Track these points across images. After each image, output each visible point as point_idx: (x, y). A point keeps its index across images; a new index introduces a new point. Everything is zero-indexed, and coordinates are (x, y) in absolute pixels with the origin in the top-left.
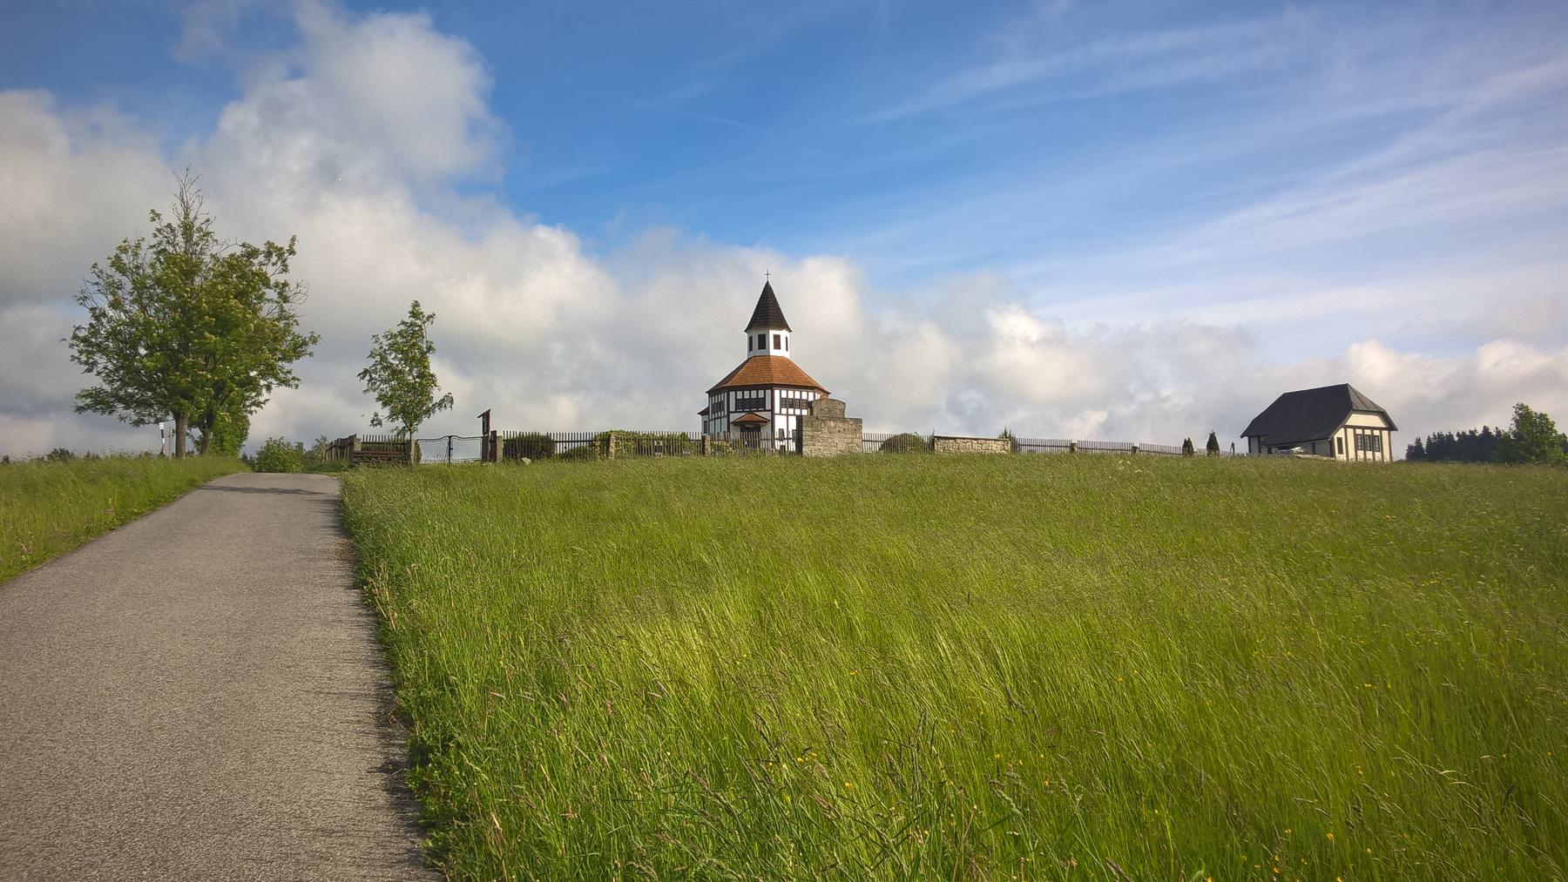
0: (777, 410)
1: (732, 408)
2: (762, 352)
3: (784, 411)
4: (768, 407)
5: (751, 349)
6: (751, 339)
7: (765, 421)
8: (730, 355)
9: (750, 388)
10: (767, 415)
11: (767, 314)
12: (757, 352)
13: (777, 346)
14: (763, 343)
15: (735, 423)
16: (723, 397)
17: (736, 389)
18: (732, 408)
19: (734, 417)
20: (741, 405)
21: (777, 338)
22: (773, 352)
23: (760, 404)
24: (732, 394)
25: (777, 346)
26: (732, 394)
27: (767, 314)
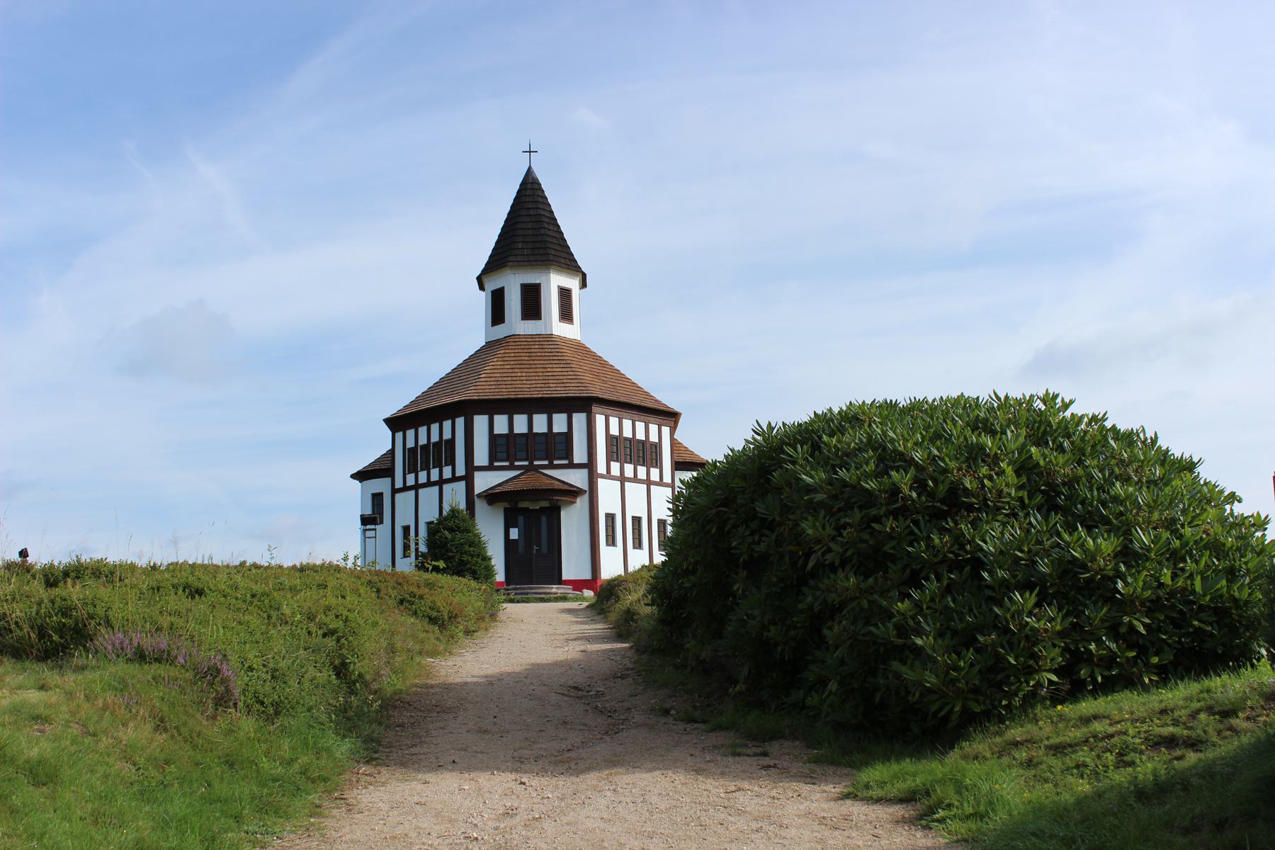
0: (601, 468)
1: (481, 457)
2: (530, 327)
3: (615, 467)
4: (579, 455)
5: (498, 315)
7: (572, 493)
8: (444, 325)
9: (530, 406)
10: (577, 478)
11: (530, 235)
12: (516, 324)
13: (566, 315)
14: (532, 307)
15: (492, 497)
16: (453, 429)
17: (491, 407)
18: (481, 457)
19: (483, 482)
20: (503, 448)
21: (565, 294)
22: (560, 329)
23: (558, 447)
24: (480, 422)
25: (566, 315)
26: (480, 422)
27: (530, 235)
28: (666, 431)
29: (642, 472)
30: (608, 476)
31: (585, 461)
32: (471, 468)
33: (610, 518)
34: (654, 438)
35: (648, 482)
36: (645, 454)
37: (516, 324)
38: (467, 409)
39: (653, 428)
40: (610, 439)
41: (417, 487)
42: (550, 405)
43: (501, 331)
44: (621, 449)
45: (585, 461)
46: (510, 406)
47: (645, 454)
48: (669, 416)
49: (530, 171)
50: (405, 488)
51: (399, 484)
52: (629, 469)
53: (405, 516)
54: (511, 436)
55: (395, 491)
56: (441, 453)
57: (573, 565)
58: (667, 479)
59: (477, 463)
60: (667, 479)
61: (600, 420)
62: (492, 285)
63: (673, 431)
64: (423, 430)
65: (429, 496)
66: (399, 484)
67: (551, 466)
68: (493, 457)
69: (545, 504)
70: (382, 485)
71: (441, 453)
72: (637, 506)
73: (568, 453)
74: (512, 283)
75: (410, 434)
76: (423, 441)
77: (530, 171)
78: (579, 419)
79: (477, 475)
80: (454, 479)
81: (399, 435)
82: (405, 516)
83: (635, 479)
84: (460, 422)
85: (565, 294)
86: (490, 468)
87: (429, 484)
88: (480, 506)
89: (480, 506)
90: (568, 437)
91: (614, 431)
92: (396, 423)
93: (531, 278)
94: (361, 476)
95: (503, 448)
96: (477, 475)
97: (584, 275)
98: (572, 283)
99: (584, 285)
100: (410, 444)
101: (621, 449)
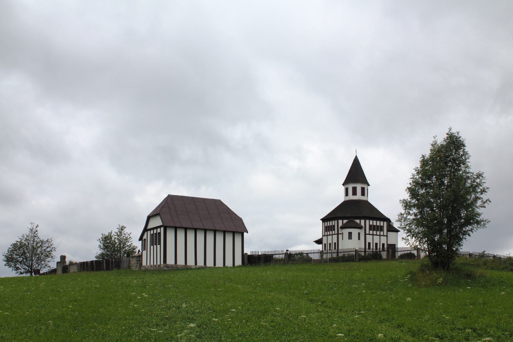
5: (347, 194)
6: (347, 190)
11: (356, 175)
13: (363, 194)
14: (354, 193)
21: (363, 189)
25: (363, 194)
28: (385, 223)
29: (378, 233)
30: (369, 234)
33: (369, 244)
34: (382, 224)
36: (381, 228)
37: (351, 197)
38: (337, 218)
40: (370, 226)
43: (348, 198)
44: (372, 228)
47: (381, 228)
49: (356, 157)
52: (375, 233)
58: (385, 234)
65: (330, 237)
74: (350, 187)
75: (326, 223)
77: (356, 157)
80: (335, 234)
83: (376, 235)
84: (336, 221)
85: (363, 189)
87: (330, 235)
91: (371, 223)
93: (354, 185)
100: (326, 225)
101: (372, 228)
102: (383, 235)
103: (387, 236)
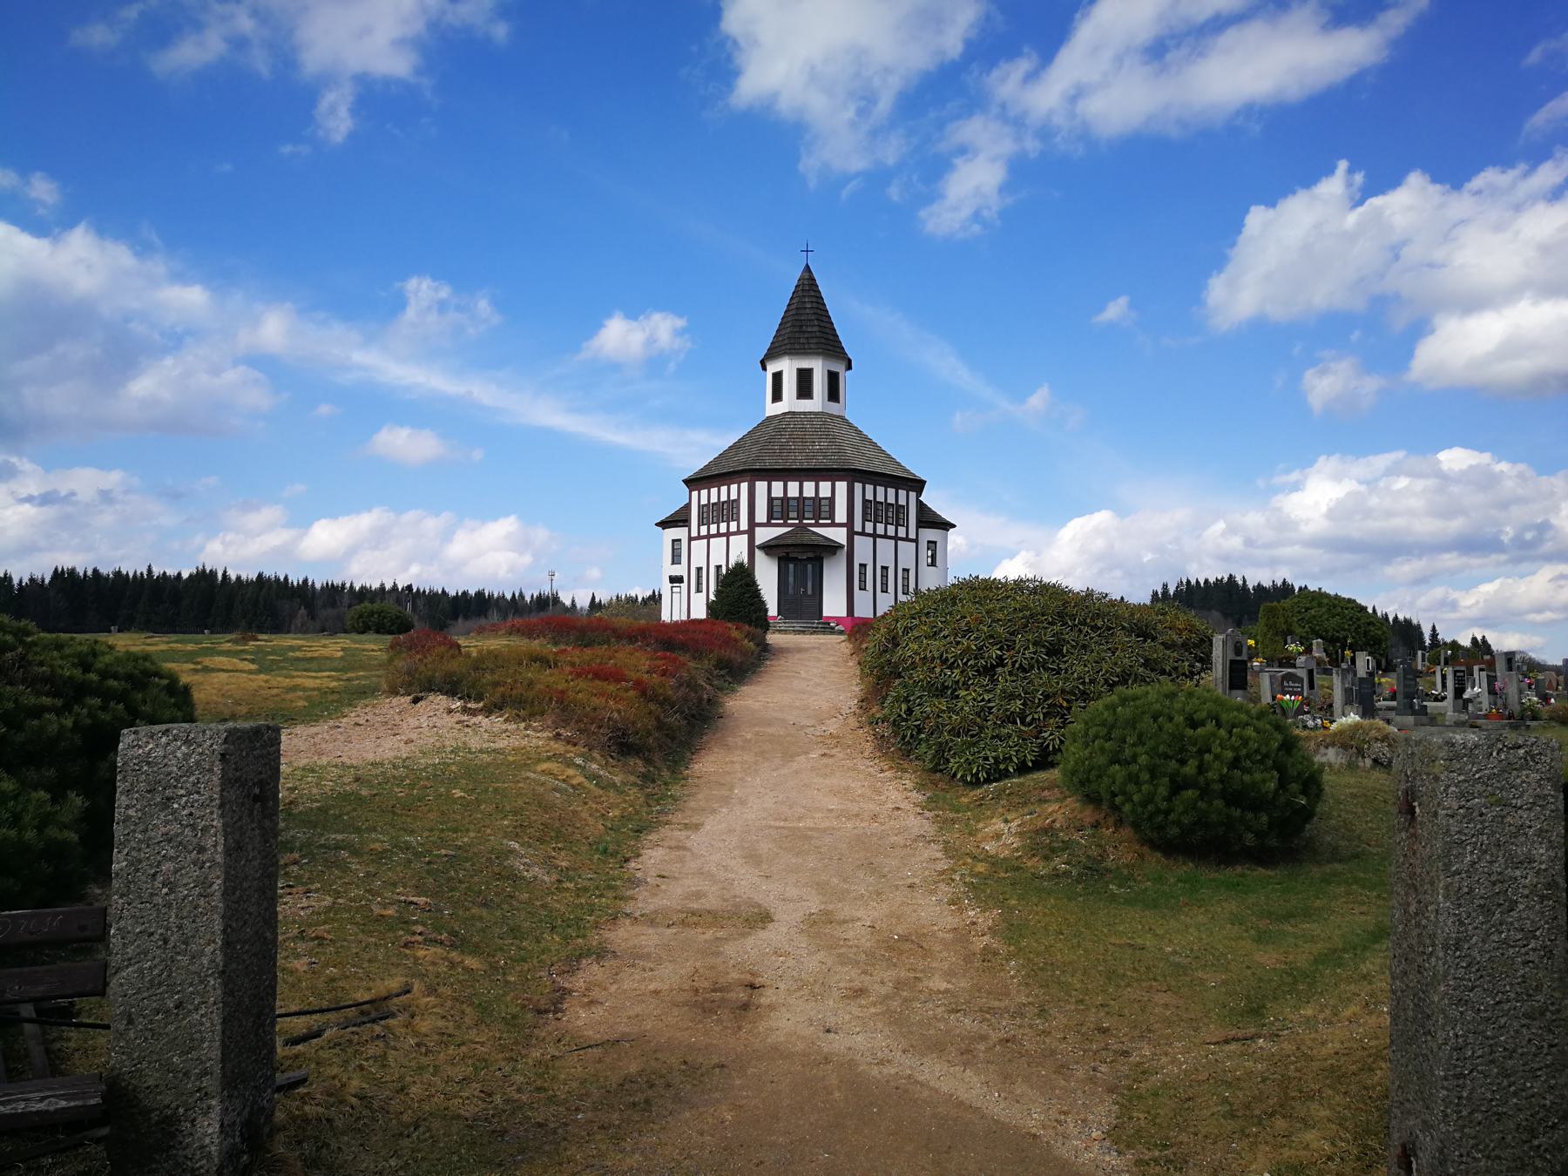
0: (858, 528)
1: (761, 515)
4: (841, 515)
7: (832, 548)
9: (802, 474)
10: (839, 535)
13: (833, 394)
15: (768, 548)
16: (738, 491)
17: (770, 474)
19: (764, 535)
24: (761, 486)
26: (761, 486)
28: (913, 495)
30: (863, 533)
31: (844, 520)
32: (753, 524)
34: (902, 502)
35: (874, 536)
39: (902, 493)
40: (865, 502)
41: (709, 537)
42: (817, 474)
44: (873, 510)
45: (844, 520)
46: (785, 474)
48: (918, 485)
50: (699, 537)
51: (694, 534)
53: (698, 560)
54: (785, 499)
55: (691, 539)
56: (727, 511)
57: (834, 604)
58: (912, 535)
59: (757, 520)
60: (912, 535)
61: (858, 486)
62: (772, 368)
63: (919, 493)
64: (714, 491)
65: (718, 544)
66: (694, 534)
67: (817, 525)
68: (770, 516)
69: (811, 555)
70: (679, 533)
71: (727, 511)
72: (885, 558)
73: (832, 515)
74: (788, 367)
76: (714, 499)
78: (842, 487)
79: (757, 529)
80: (739, 532)
81: (695, 494)
82: (698, 560)
83: (885, 536)
84: (744, 486)
85: (833, 379)
86: (768, 524)
87: (719, 535)
88: (759, 554)
89: (759, 554)
90: (832, 500)
91: (869, 496)
92: (694, 482)
94: (664, 524)
95: (780, 509)
96: (757, 529)
97: (850, 361)
98: (838, 367)
99: (849, 367)
101: (873, 510)
102: (907, 539)
103: (916, 541)
